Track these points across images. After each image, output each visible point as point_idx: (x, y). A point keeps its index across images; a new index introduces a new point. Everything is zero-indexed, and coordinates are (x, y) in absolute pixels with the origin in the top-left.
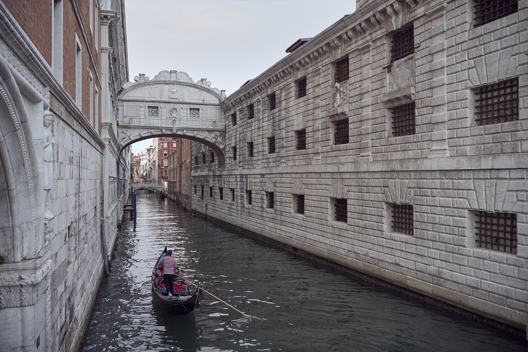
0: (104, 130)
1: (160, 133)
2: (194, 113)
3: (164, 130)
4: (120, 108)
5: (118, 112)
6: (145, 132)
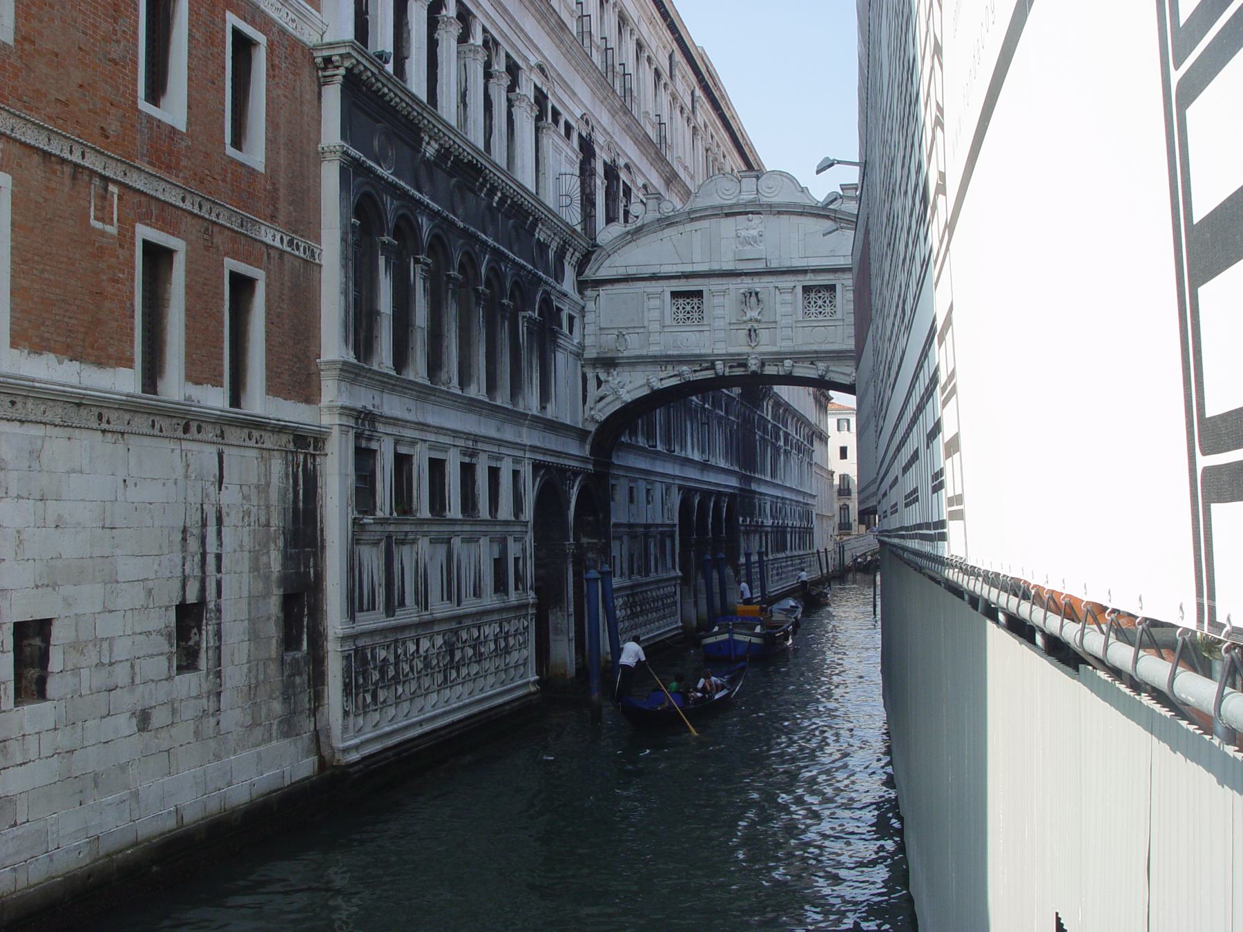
0: (330, 383)
1: (709, 374)
2: (820, 302)
3: (719, 366)
4: (590, 305)
5: (584, 317)
6: (663, 375)
